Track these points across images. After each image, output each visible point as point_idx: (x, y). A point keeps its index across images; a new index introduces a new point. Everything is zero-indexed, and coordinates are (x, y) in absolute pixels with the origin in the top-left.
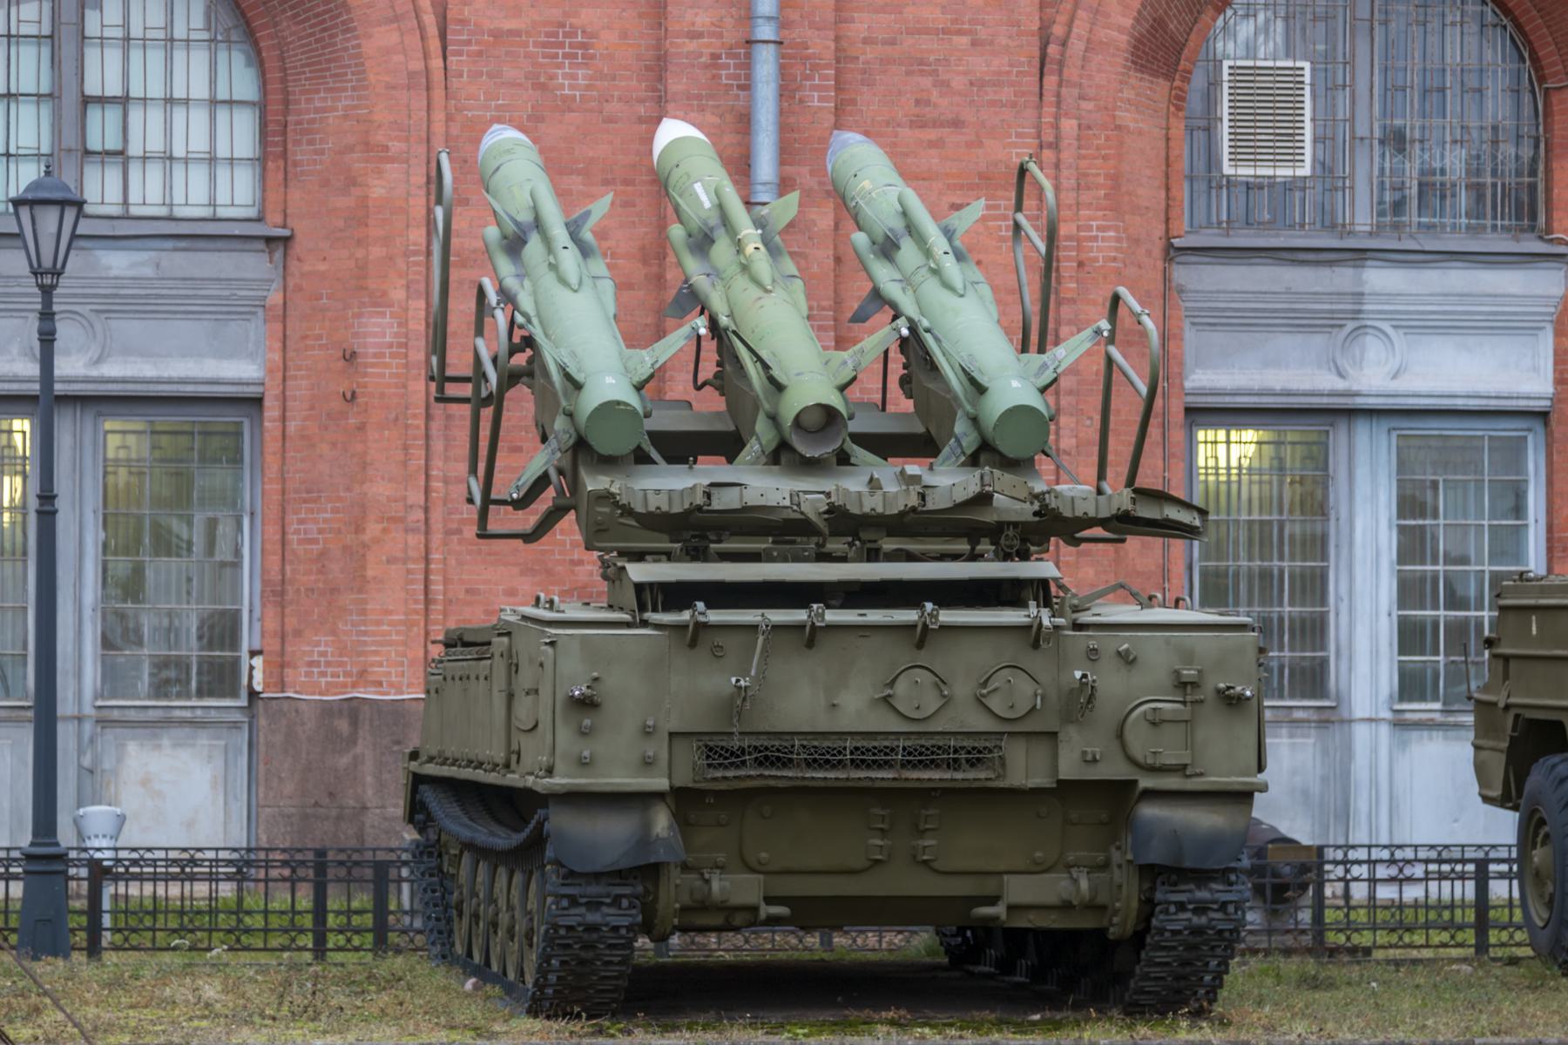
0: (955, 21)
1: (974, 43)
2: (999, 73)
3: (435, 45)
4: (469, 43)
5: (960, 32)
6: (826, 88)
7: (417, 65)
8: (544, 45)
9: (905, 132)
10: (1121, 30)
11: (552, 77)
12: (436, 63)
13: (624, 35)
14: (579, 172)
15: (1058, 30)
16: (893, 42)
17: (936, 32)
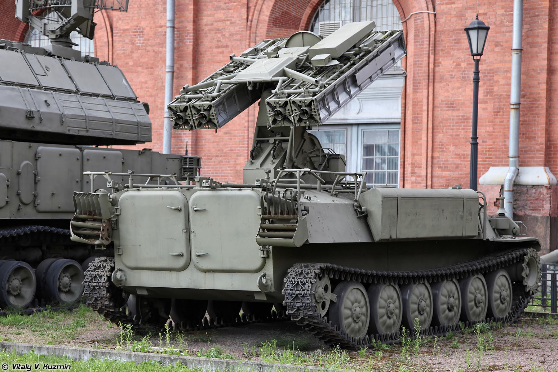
0: (226, 17)
1: (231, 23)
2: (237, 31)
3: (110, 34)
4: (117, 33)
5: (228, 20)
6: (190, 39)
7: (106, 40)
8: (134, 32)
9: (215, 50)
10: (266, 16)
11: (135, 41)
12: (110, 39)
13: (151, 28)
14: (140, 66)
15: (250, 18)
16: (212, 25)
17: (223, 21)
